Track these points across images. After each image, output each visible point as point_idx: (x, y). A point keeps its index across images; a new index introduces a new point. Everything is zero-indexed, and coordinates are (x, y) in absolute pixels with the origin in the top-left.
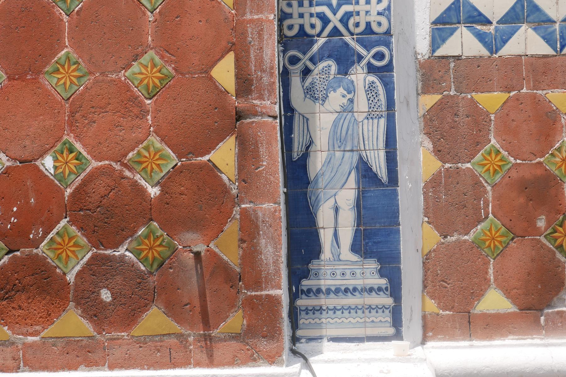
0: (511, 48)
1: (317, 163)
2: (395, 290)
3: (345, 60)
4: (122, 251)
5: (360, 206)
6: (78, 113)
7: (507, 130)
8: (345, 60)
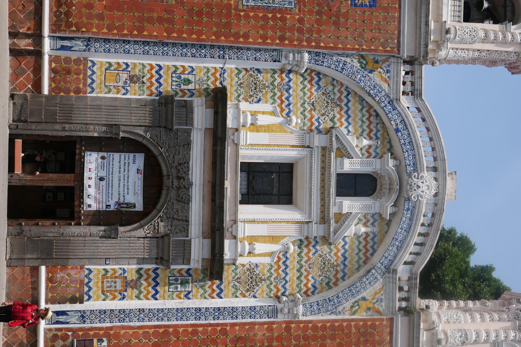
0: (88, 70)
1: (74, 42)
2: (56, 50)
4: (63, 16)
6: (80, 12)
7: (77, 69)
8: (87, 46)
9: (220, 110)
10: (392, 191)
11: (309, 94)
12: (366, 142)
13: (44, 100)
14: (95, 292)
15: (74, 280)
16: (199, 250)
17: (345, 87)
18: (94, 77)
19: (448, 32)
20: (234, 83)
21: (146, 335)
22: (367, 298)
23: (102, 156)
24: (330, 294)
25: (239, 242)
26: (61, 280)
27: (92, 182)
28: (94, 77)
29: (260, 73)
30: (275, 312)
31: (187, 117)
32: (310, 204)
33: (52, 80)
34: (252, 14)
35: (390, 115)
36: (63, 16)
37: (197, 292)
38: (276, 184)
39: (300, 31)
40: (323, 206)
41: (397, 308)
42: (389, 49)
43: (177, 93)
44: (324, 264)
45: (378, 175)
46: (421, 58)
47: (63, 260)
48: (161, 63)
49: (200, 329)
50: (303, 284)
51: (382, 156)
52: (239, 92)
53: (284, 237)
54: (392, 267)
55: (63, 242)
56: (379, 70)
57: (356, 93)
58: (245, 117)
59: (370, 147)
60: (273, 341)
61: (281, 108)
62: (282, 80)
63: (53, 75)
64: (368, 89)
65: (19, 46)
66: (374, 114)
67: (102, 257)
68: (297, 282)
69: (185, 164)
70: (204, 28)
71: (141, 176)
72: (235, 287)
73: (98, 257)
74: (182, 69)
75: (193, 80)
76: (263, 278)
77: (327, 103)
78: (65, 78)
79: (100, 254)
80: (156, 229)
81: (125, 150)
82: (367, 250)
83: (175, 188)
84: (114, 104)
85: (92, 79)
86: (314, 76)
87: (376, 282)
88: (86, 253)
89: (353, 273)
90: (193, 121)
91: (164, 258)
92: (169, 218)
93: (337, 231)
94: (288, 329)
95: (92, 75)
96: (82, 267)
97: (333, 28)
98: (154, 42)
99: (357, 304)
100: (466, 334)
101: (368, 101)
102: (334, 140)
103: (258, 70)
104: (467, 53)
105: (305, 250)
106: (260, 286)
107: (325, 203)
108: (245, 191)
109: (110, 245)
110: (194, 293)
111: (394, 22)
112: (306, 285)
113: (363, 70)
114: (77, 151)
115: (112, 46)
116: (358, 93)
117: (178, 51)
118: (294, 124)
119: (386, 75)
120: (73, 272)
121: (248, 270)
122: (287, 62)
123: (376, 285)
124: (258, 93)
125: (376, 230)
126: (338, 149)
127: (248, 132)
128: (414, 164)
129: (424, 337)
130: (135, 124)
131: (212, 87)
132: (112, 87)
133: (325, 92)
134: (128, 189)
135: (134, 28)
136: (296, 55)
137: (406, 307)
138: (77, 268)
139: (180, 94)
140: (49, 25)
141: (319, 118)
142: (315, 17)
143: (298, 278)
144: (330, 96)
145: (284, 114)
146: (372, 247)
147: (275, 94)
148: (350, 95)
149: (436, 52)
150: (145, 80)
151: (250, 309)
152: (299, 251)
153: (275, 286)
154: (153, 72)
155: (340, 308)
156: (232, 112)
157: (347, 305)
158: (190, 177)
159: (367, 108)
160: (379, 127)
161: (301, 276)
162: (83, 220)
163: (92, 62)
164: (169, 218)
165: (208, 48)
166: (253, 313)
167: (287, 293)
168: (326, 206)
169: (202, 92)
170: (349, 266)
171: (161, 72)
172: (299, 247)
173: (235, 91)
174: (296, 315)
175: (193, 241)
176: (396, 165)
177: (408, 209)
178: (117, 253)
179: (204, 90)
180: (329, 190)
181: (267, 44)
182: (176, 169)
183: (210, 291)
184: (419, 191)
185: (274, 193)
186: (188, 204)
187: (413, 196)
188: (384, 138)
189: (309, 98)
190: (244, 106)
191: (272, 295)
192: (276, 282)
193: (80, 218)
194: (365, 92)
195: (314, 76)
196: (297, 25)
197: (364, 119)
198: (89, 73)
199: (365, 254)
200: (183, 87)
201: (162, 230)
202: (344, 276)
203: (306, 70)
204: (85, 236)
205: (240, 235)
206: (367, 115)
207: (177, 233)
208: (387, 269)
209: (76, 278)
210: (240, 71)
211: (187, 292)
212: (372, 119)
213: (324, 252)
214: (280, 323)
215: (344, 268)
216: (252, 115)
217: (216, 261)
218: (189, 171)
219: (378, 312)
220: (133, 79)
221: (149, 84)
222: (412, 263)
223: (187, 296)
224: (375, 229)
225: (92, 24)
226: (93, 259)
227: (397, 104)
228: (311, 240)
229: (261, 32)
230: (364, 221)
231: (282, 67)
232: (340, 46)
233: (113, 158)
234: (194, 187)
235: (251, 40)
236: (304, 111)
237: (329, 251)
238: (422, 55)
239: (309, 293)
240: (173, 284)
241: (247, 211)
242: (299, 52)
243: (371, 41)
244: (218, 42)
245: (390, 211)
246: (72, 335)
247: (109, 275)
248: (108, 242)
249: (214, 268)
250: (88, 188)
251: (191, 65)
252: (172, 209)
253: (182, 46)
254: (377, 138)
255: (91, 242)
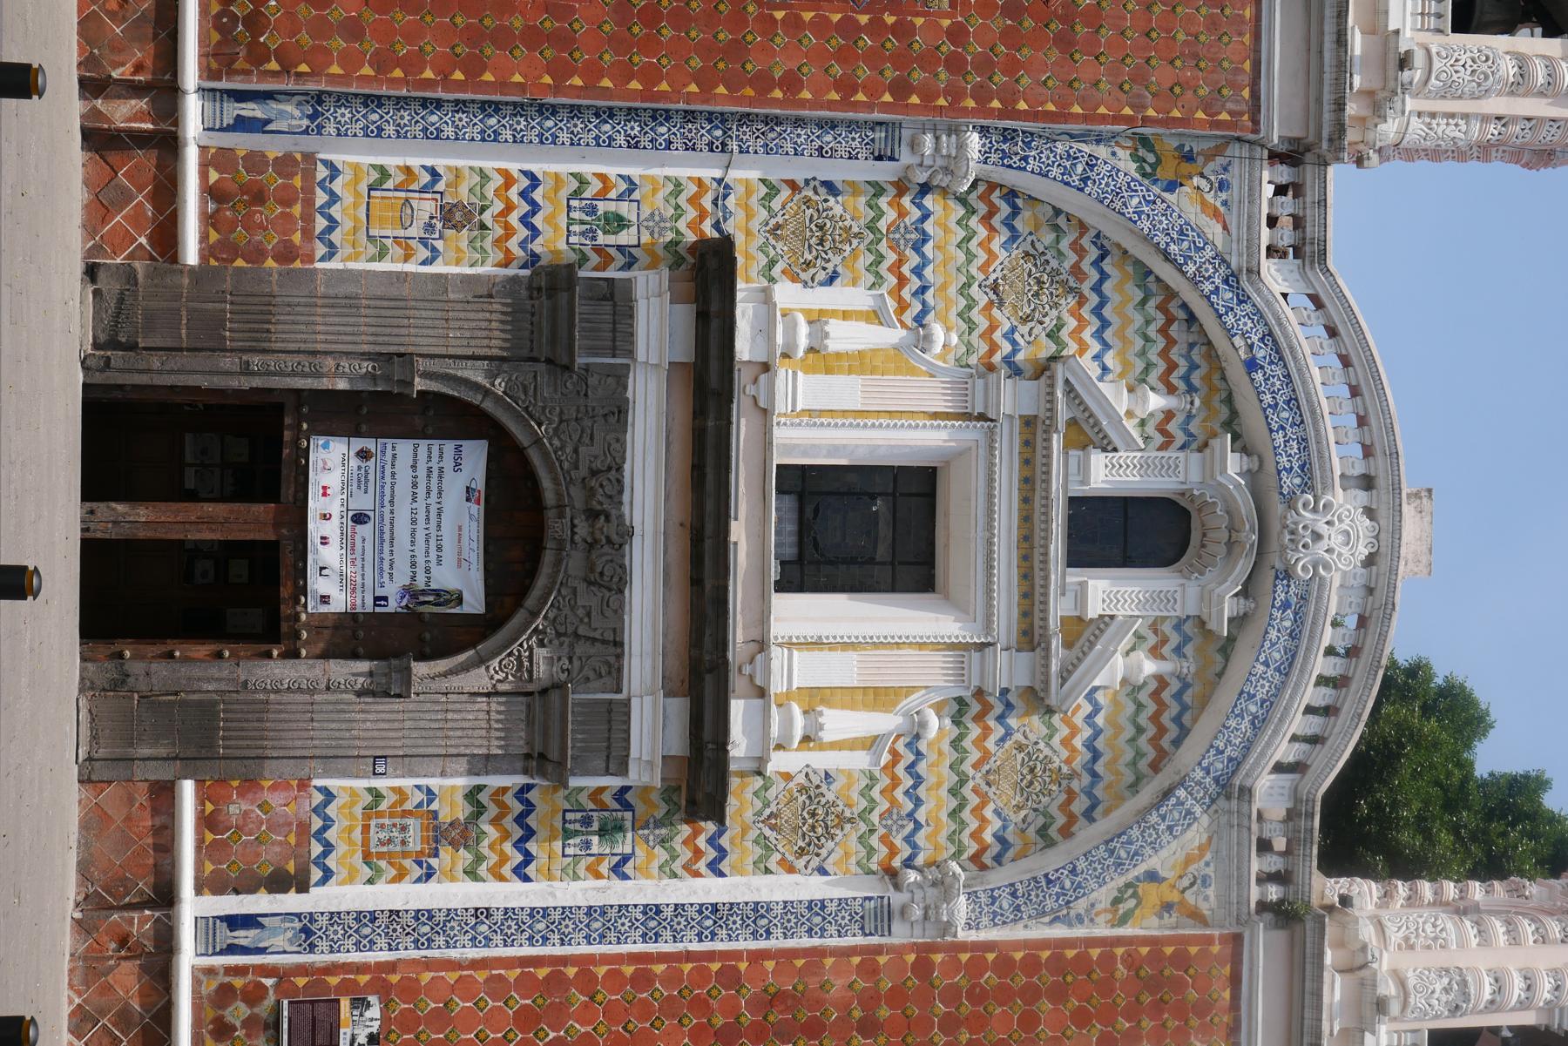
0: (319, 191)
1: (273, 105)
2: (221, 129)
3: (312, 118)
4: (240, 27)
5: (255, 119)
6: (291, 15)
7: (285, 187)
8: (312, 118)
9: (714, 307)
10: (1237, 549)
11: (982, 257)
12: (1156, 402)
13: (186, 281)
14: (344, 856)
15: (281, 821)
16: (653, 729)
17: (1092, 233)
18: (335, 211)
19: (1404, 62)
20: (755, 225)
21: (497, 987)
22: (1162, 873)
23: (361, 450)
24: (1052, 861)
25: (774, 707)
26: (241, 822)
27: (332, 529)
28: (335, 211)
29: (835, 195)
30: (883, 916)
31: (614, 330)
32: (989, 592)
33: (209, 221)
34: (808, 16)
35: (1230, 319)
36: (240, 27)
37: (650, 857)
38: (884, 531)
39: (955, 64)
40: (1027, 595)
41: (1253, 905)
42: (1224, 116)
43: (584, 259)
44: (1032, 770)
45: (1192, 501)
46: (1325, 145)
47: (246, 762)
48: (535, 168)
49: (659, 968)
50: (967, 832)
51: (1206, 445)
52: (772, 253)
53: (911, 690)
54: (1237, 781)
55: (245, 707)
56: (1196, 180)
57: (1125, 252)
58: (792, 329)
59: (1169, 415)
60: (878, 1006)
61: (900, 300)
62: (902, 214)
63: (211, 207)
64: (1161, 239)
65: (108, 120)
66: (1181, 315)
67: (363, 753)
68: (948, 826)
69: (610, 472)
70: (664, 61)
71: (477, 510)
72: (762, 841)
73: (350, 753)
74: (601, 185)
75: (634, 218)
76: (848, 814)
77: (1039, 282)
78: (249, 215)
79: (357, 743)
80: (524, 668)
81: (430, 431)
82: (1162, 730)
83: (581, 545)
84: (394, 292)
85: (330, 219)
86: (997, 202)
87: (1189, 825)
88: (316, 742)
89: (1121, 799)
90: (632, 343)
91: (550, 756)
92: (565, 636)
93: (1070, 673)
94: (923, 967)
95: (330, 204)
96: (304, 785)
97: (1055, 54)
98: (515, 104)
99: (1130, 891)
100: (1464, 983)
101: (1162, 276)
102: (1059, 395)
103: (830, 187)
104: (1464, 128)
105: (975, 731)
106: (837, 839)
107: (1032, 586)
108: (790, 552)
109: (387, 716)
110: (638, 861)
111: (1240, 34)
112: (975, 836)
113: (1146, 182)
114: (287, 435)
115: (389, 119)
116: (1131, 251)
117: (587, 130)
118: (938, 348)
119: (1216, 196)
120: (275, 799)
121: (802, 789)
122: (915, 160)
123: (1190, 834)
124: (830, 254)
125: (1188, 667)
126: (1072, 423)
127: (800, 374)
128: (1302, 467)
129: (1335, 990)
130: (459, 352)
131: (691, 237)
132: (388, 242)
133: (1032, 252)
134: (439, 548)
135: (455, 61)
136: (944, 138)
137: (1281, 902)
138: (288, 787)
139: (595, 259)
140: (200, 56)
141: (1013, 329)
142: (999, 23)
143: (954, 814)
144: (1047, 262)
145: (908, 317)
146: (1177, 720)
147: (880, 258)
148: (1108, 260)
149: (1370, 124)
150: (487, 217)
151: (810, 908)
152: (956, 731)
153: (884, 840)
154: (513, 194)
155: (1080, 906)
156: (751, 312)
157: (1103, 895)
158: (626, 509)
159: (1159, 299)
160: (1196, 355)
161: (961, 807)
162: (307, 642)
163: (330, 165)
164: (565, 634)
165: (678, 119)
166: (817, 920)
167: (920, 860)
168: (1037, 597)
169: (660, 252)
170: (1108, 777)
171: (537, 195)
172: (957, 722)
173: (761, 249)
174: (948, 927)
175: (635, 703)
176: (1249, 471)
177: (1286, 605)
178: (408, 742)
179: (666, 247)
180: (1046, 547)
181: (856, 106)
182: (584, 487)
183: (689, 855)
184: (1320, 549)
185: (878, 558)
186: (621, 592)
187: (1302, 564)
188: (1212, 389)
189: (984, 268)
190: (787, 294)
191: (874, 867)
192: (885, 826)
193: (297, 636)
194: (1153, 250)
195: (999, 202)
196: (944, 49)
197: (1152, 331)
198: (321, 198)
199: (1154, 741)
200: (602, 239)
201: (542, 670)
202: (1093, 807)
203: (974, 185)
204: (311, 691)
205: (777, 686)
206: (1160, 320)
207: (588, 679)
208: (1223, 786)
209: (286, 814)
210: (773, 191)
211: (617, 858)
212: (1174, 330)
213: (1030, 736)
214: (898, 951)
215: (1093, 785)
216: (810, 322)
217: (706, 764)
218: (621, 492)
219: (1196, 916)
220: (452, 216)
221: (500, 231)
222: (1297, 768)
223: (618, 870)
224: (1185, 664)
225: (328, 52)
226: (334, 760)
227: (1252, 284)
228: (991, 700)
229: (837, 70)
230: (1152, 640)
231: (901, 175)
232: (1077, 109)
233: (394, 456)
234: (636, 540)
235: (806, 94)
236: (969, 308)
237: (1045, 731)
238: (1325, 134)
239: (987, 859)
240: (576, 833)
241: (797, 614)
242: (953, 130)
243: (1170, 94)
244: (706, 101)
245: (1231, 609)
246: (277, 986)
247: (384, 806)
248: (380, 708)
249: (701, 785)
250: (320, 547)
251: (625, 171)
252: (572, 609)
253: (597, 115)
254: (1191, 389)
255: (331, 707)
